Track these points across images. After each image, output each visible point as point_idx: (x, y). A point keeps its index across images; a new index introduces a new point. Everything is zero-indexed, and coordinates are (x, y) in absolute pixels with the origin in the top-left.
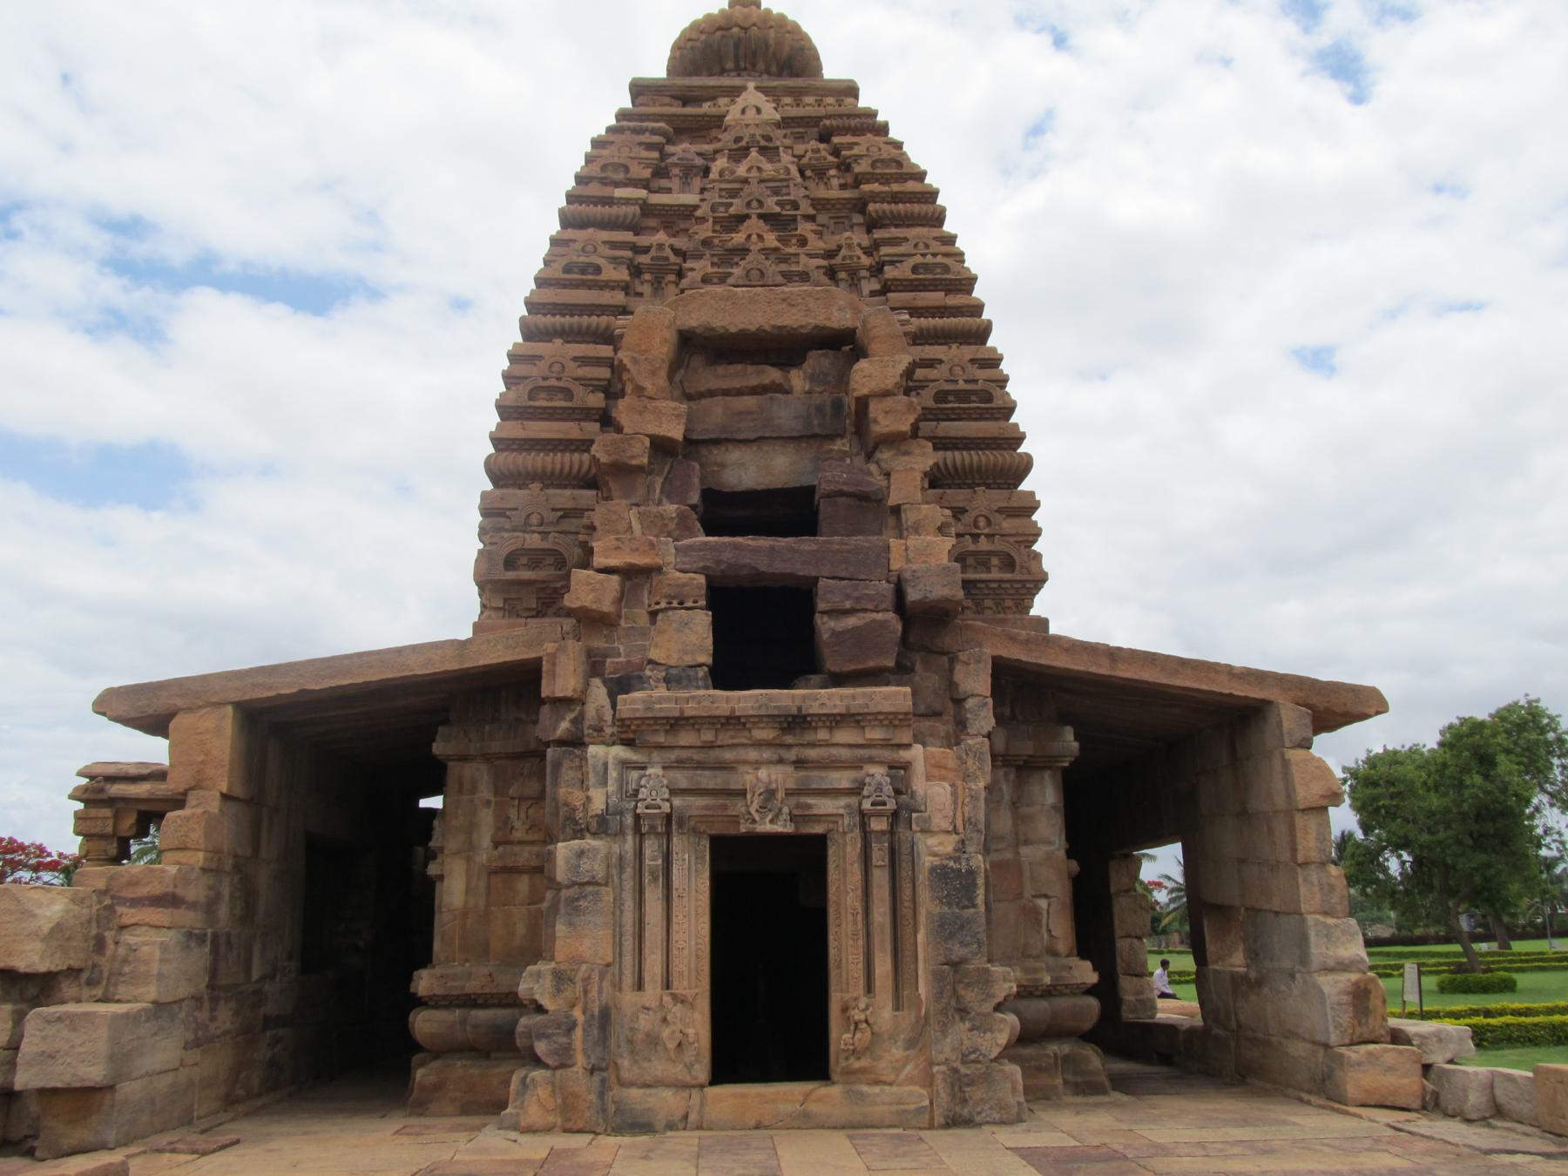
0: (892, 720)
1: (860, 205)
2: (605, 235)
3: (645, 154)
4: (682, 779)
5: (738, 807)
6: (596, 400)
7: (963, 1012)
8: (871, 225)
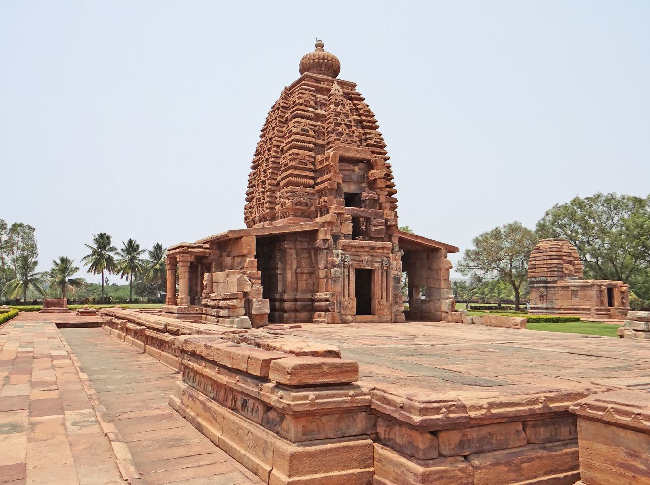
0: (388, 249)
1: (361, 121)
2: (308, 121)
3: (313, 98)
5: (361, 263)
6: (312, 167)
7: (396, 303)
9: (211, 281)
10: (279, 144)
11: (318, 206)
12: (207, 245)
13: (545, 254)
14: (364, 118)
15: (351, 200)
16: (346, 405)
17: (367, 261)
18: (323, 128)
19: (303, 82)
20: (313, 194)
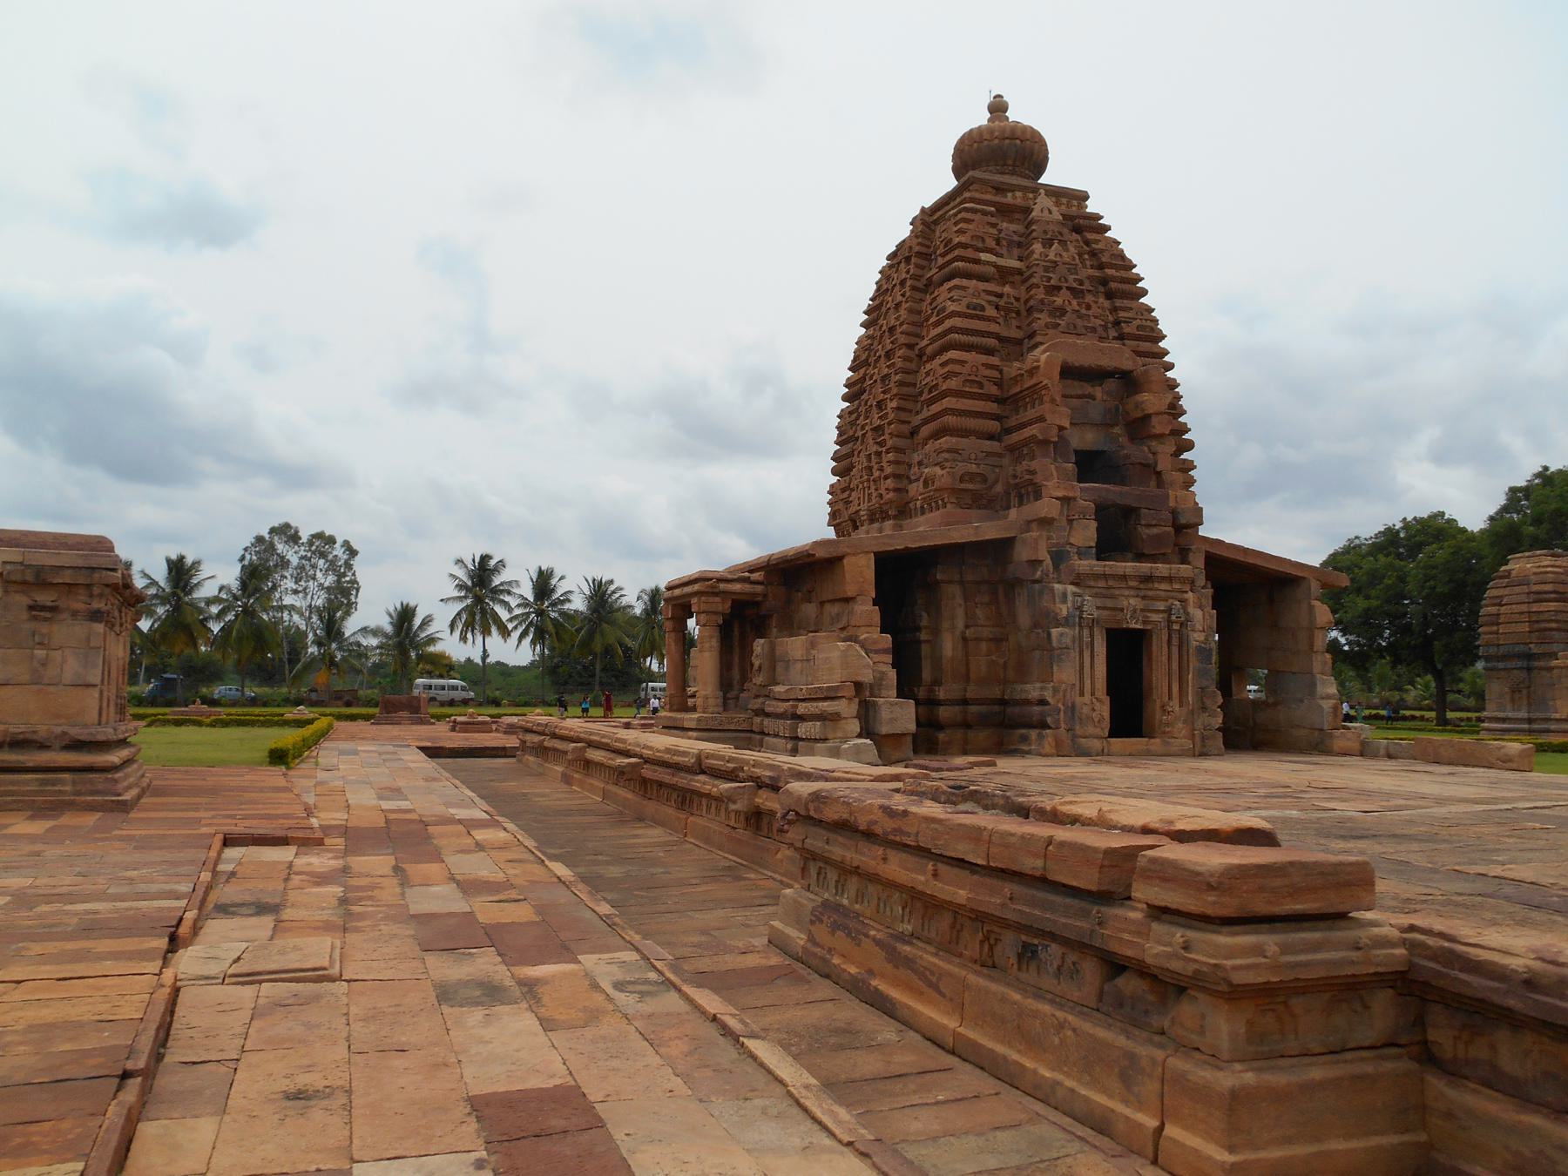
0: (1183, 580)
1: (1104, 282)
2: (983, 286)
4: (1099, 602)
5: (1120, 616)
6: (994, 390)
7: (1204, 709)
8: (1110, 295)
9: (773, 658)
10: (912, 340)
11: (1012, 482)
12: (756, 576)
13: (1525, 589)
14: (1109, 272)
15: (1089, 465)
16: (1349, 971)
17: (1135, 611)
18: (1017, 299)
19: (967, 195)
20: (999, 455)
